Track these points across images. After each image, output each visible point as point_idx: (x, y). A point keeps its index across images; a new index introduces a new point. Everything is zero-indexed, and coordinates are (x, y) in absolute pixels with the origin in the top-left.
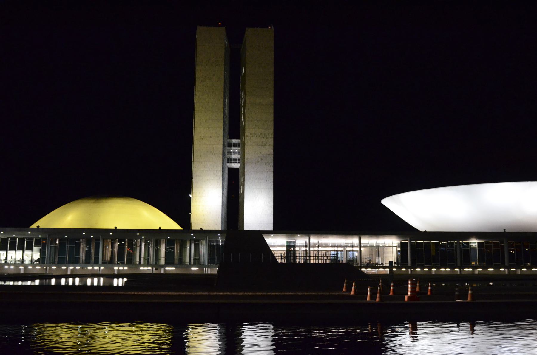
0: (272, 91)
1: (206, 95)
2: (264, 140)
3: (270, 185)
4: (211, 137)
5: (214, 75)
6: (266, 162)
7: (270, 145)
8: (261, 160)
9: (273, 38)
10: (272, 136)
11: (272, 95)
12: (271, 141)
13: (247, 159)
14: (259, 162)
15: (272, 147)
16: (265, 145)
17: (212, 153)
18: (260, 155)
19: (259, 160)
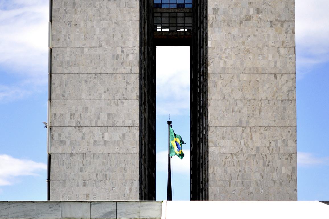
3: (285, 89)
6: (272, 18)
8: (258, 11)
13: (216, 11)
14: (249, 18)
19: (251, 12)
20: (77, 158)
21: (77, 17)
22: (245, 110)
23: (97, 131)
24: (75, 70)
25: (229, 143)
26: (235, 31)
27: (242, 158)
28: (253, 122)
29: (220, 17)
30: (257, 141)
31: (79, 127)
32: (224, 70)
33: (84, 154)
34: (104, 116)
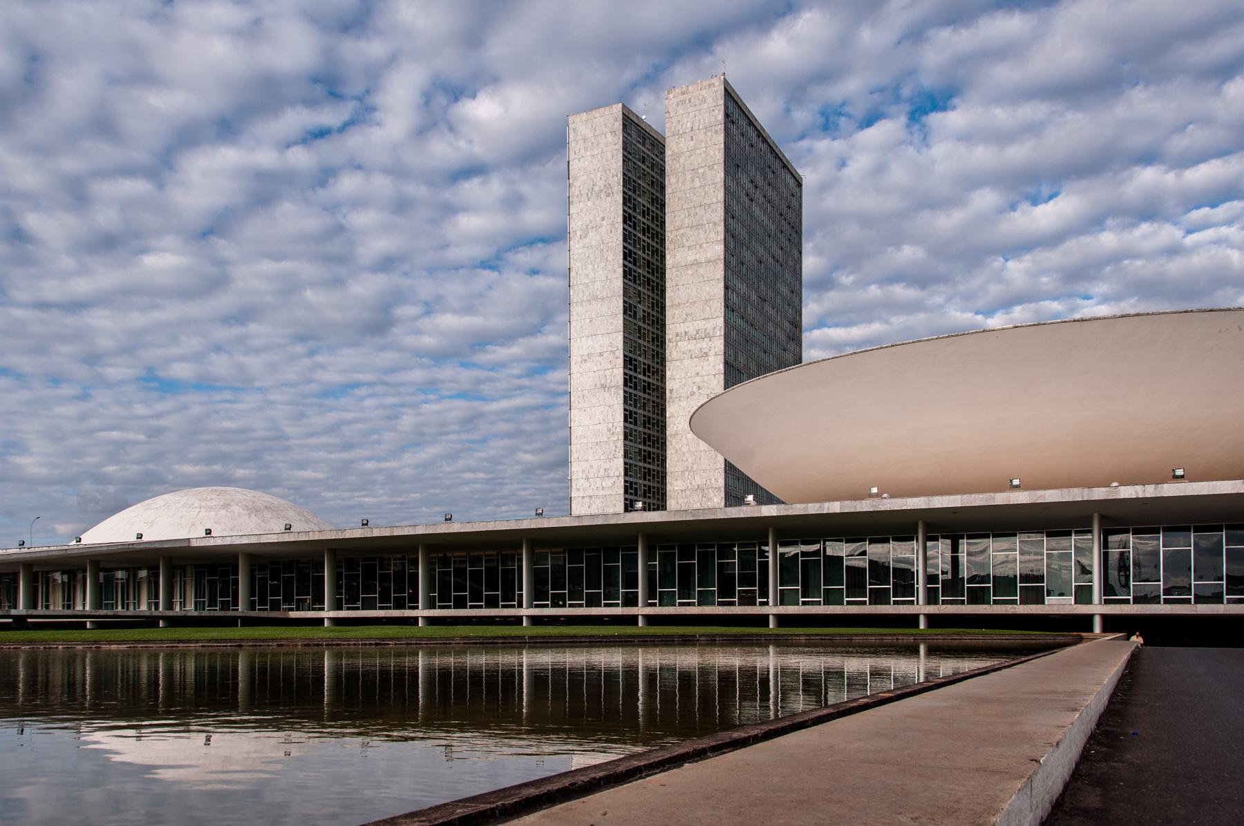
0: (721, 229)
1: (590, 267)
2: (704, 345)
4: (601, 354)
5: (603, 219)
7: (716, 354)
8: (699, 388)
9: (722, 102)
10: (720, 332)
11: (722, 237)
12: (719, 344)
13: (671, 391)
14: (693, 394)
15: (721, 359)
16: (706, 354)
17: (603, 387)
18: (698, 379)
19: (695, 389)
20: (587, 499)
21: (586, 405)
22: (690, 460)
23: (598, 481)
24: (585, 441)
25: (679, 483)
26: (684, 404)
27: (688, 493)
28: (695, 467)
29: (674, 395)
30: (698, 481)
31: (587, 479)
32: (677, 433)
33: (590, 497)
34: (602, 470)
